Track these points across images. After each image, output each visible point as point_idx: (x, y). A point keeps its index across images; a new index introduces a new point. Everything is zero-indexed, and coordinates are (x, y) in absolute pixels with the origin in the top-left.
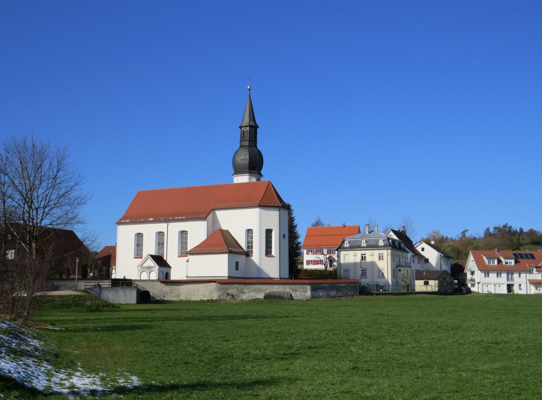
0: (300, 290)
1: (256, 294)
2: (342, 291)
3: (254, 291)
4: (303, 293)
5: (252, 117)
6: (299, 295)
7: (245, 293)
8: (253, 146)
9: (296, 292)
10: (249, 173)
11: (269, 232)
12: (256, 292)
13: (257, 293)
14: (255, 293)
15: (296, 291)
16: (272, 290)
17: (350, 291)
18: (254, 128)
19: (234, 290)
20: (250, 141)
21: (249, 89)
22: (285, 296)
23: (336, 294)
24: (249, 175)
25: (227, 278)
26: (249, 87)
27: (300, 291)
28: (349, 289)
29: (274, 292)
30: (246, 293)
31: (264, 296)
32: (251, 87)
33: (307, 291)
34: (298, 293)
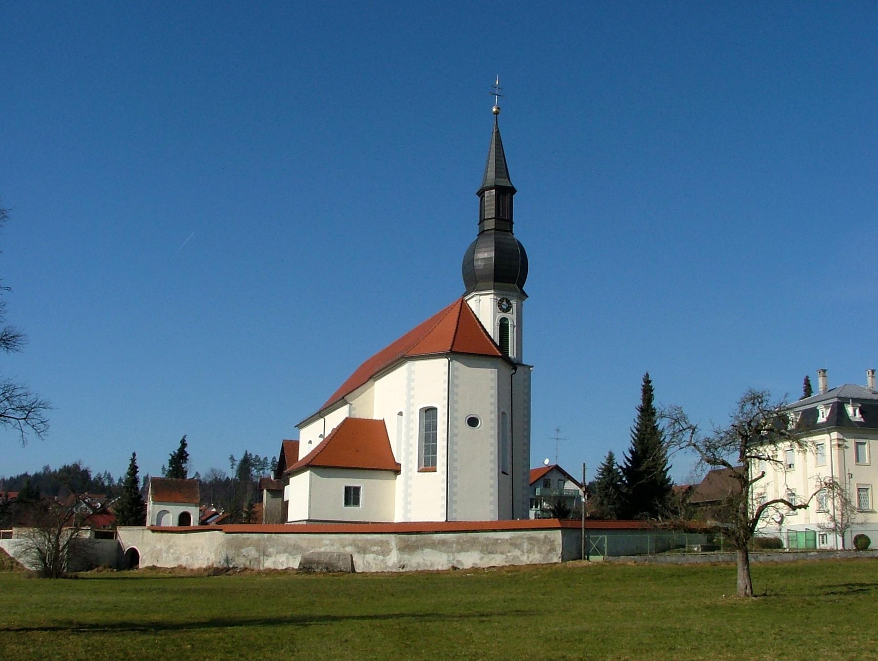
0: (375, 548)
1: (288, 559)
2: (502, 553)
3: (285, 551)
4: (381, 557)
5: (502, 168)
6: (371, 561)
7: (269, 556)
8: (508, 231)
9: (365, 553)
10: (494, 289)
11: (429, 413)
12: (290, 553)
13: (291, 557)
14: (286, 554)
15: (363, 550)
16: (318, 550)
17: (529, 552)
18: (505, 193)
19: (251, 548)
20: (500, 220)
21: (497, 113)
23: (481, 559)
24: (494, 294)
25: (305, 523)
26: (494, 110)
27: (374, 552)
28: (526, 546)
29: (320, 554)
30: (271, 557)
32: (499, 108)
33: (390, 551)
34: (370, 557)
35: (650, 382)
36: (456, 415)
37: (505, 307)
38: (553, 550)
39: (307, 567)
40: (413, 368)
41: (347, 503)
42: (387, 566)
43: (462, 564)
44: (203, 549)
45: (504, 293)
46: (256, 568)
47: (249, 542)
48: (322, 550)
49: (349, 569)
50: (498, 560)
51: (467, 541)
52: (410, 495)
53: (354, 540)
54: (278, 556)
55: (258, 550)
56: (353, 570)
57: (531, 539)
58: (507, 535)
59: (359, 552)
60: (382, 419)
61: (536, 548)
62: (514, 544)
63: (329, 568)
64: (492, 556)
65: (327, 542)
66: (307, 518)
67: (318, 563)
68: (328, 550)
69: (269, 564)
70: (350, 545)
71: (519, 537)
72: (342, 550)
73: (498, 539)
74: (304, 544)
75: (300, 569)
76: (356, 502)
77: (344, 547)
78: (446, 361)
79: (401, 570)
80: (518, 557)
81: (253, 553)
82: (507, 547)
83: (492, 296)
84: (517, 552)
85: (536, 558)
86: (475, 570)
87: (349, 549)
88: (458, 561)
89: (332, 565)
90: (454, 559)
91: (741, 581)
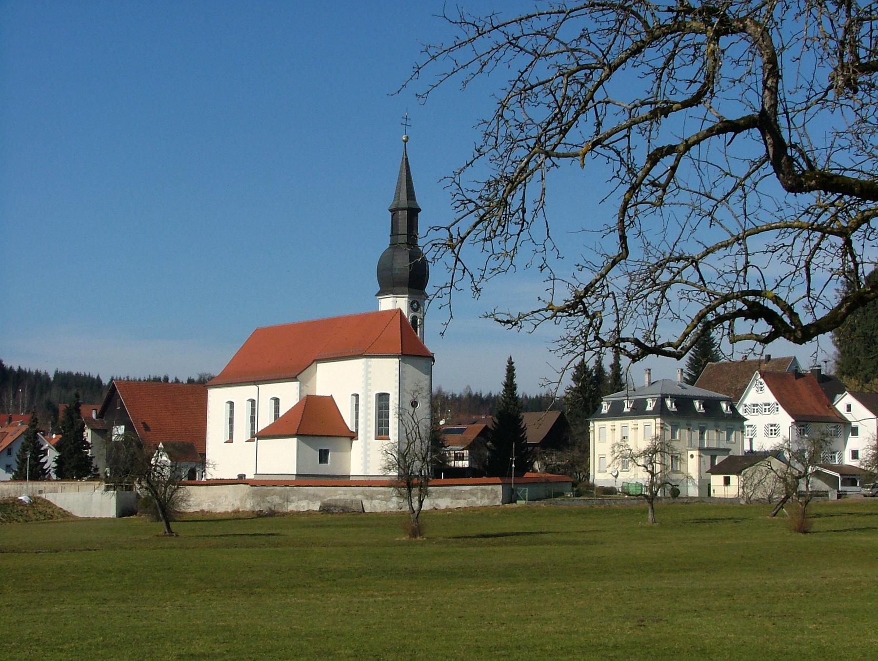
0: (380, 496)
1: (308, 503)
2: (465, 499)
3: (306, 499)
6: (377, 505)
7: (292, 502)
9: (372, 500)
11: (383, 399)
12: (310, 500)
13: (311, 503)
14: (307, 501)
15: (371, 497)
16: (334, 498)
17: (482, 498)
21: (405, 141)
22: (354, 506)
23: (452, 503)
25: (294, 478)
27: (378, 499)
28: (479, 495)
29: (336, 500)
30: (293, 502)
31: (320, 507)
32: (407, 137)
34: (376, 502)
35: (513, 363)
36: (404, 400)
37: (415, 307)
38: (496, 497)
39: (326, 509)
40: (369, 363)
41: (321, 462)
42: (390, 508)
43: (440, 506)
44: (226, 497)
45: (414, 296)
46: (280, 510)
47: (272, 492)
48: (338, 497)
49: (361, 510)
50: (462, 504)
51: (442, 492)
52: (369, 455)
53: (363, 491)
54: (299, 502)
55: (281, 498)
56: (364, 511)
57: (482, 490)
58: (468, 488)
59: (367, 499)
60: (330, 395)
61: (486, 496)
62: (472, 494)
63: (345, 510)
64: (459, 501)
65: (342, 492)
66: (295, 473)
67: (335, 506)
68: (342, 498)
69: (291, 507)
70: (360, 494)
71: (475, 489)
72: (353, 497)
73: (462, 490)
74: (322, 494)
75: (320, 511)
76: (326, 461)
77: (355, 495)
78: (397, 360)
79: (399, 510)
80: (475, 502)
81: (277, 500)
82: (468, 496)
83: (407, 299)
84: (474, 499)
85: (486, 502)
86: (448, 509)
87: (359, 497)
88: (437, 504)
89: (346, 508)
90: (434, 503)
91: (650, 517)
